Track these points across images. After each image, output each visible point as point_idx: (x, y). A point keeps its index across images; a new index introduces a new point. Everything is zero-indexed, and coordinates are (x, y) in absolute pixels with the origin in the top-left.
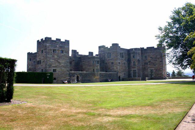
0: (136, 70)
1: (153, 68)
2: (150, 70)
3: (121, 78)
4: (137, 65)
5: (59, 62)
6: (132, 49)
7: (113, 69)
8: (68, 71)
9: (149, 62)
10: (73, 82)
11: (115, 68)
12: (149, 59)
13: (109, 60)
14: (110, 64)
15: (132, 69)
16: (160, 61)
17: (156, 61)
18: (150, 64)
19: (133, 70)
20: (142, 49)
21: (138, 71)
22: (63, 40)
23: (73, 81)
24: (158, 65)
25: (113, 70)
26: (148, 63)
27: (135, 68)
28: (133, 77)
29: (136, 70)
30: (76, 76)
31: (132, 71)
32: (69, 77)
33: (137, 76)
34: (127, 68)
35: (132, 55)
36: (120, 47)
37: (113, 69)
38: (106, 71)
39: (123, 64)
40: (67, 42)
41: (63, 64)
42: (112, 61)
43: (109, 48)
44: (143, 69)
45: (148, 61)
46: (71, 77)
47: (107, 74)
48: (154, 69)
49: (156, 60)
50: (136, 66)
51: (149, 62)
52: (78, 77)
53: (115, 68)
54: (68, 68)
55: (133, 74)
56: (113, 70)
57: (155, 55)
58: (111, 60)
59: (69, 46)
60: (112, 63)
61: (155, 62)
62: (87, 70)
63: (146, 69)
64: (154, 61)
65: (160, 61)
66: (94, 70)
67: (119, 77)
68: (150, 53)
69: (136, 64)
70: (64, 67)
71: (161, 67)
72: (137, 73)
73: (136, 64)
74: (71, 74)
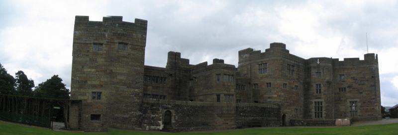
0: (321, 102)
1: (358, 98)
2: (351, 102)
3: (287, 119)
4: (325, 91)
5: (111, 73)
6: (313, 60)
7: (269, 98)
8: (137, 95)
9: (349, 87)
10: (152, 127)
11: (276, 96)
12: (349, 81)
13: (262, 78)
14: (264, 86)
15: (314, 101)
16: (372, 86)
17: (363, 84)
18: (350, 92)
19: (315, 102)
20: (334, 62)
21: (327, 104)
22: (129, 19)
23: (151, 124)
24: (366, 92)
25: (269, 100)
26: (347, 90)
27: (320, 98)
28: (316, 117)
29: (321, 102)
30: (162, 111)
31: (314, 105)
32: (139, 113)
33: (324, 115)
34: (302, 98)
35: (313, 72)
36: (288, 51)
37: (269, 98)
38: (257, 102)
39: (293, 88)
40: (141, 26)
41: (122, 78)
42: (267, 81)
43: (263, 54)
44: (336, 101)
45: (348, 85)
46: (145, 112)
47: (256, 107)
48: (358, 100)
49: (362, 83)
50: (322, 94)
51: (349, 87)
52: (168, 114)
53: (276, 96)
54: (138, 88)
55: (316, 110)
56: (269, 100)
57: (361, 73)
58: (267, 77)
59: (146, 34)
60: (269, 84)
61: (361, 86)
62: (201, 98)
63: (342, 100)
64: (359, 85)
65: (372, 86)
66: (218, 96)
67: (284, 116)
68: (351, 69)
69: (322, 91)
70: (124, 84)
71: (374, 97)
72: (323, 109)
73: (323, 89)
74: (148, 104)
